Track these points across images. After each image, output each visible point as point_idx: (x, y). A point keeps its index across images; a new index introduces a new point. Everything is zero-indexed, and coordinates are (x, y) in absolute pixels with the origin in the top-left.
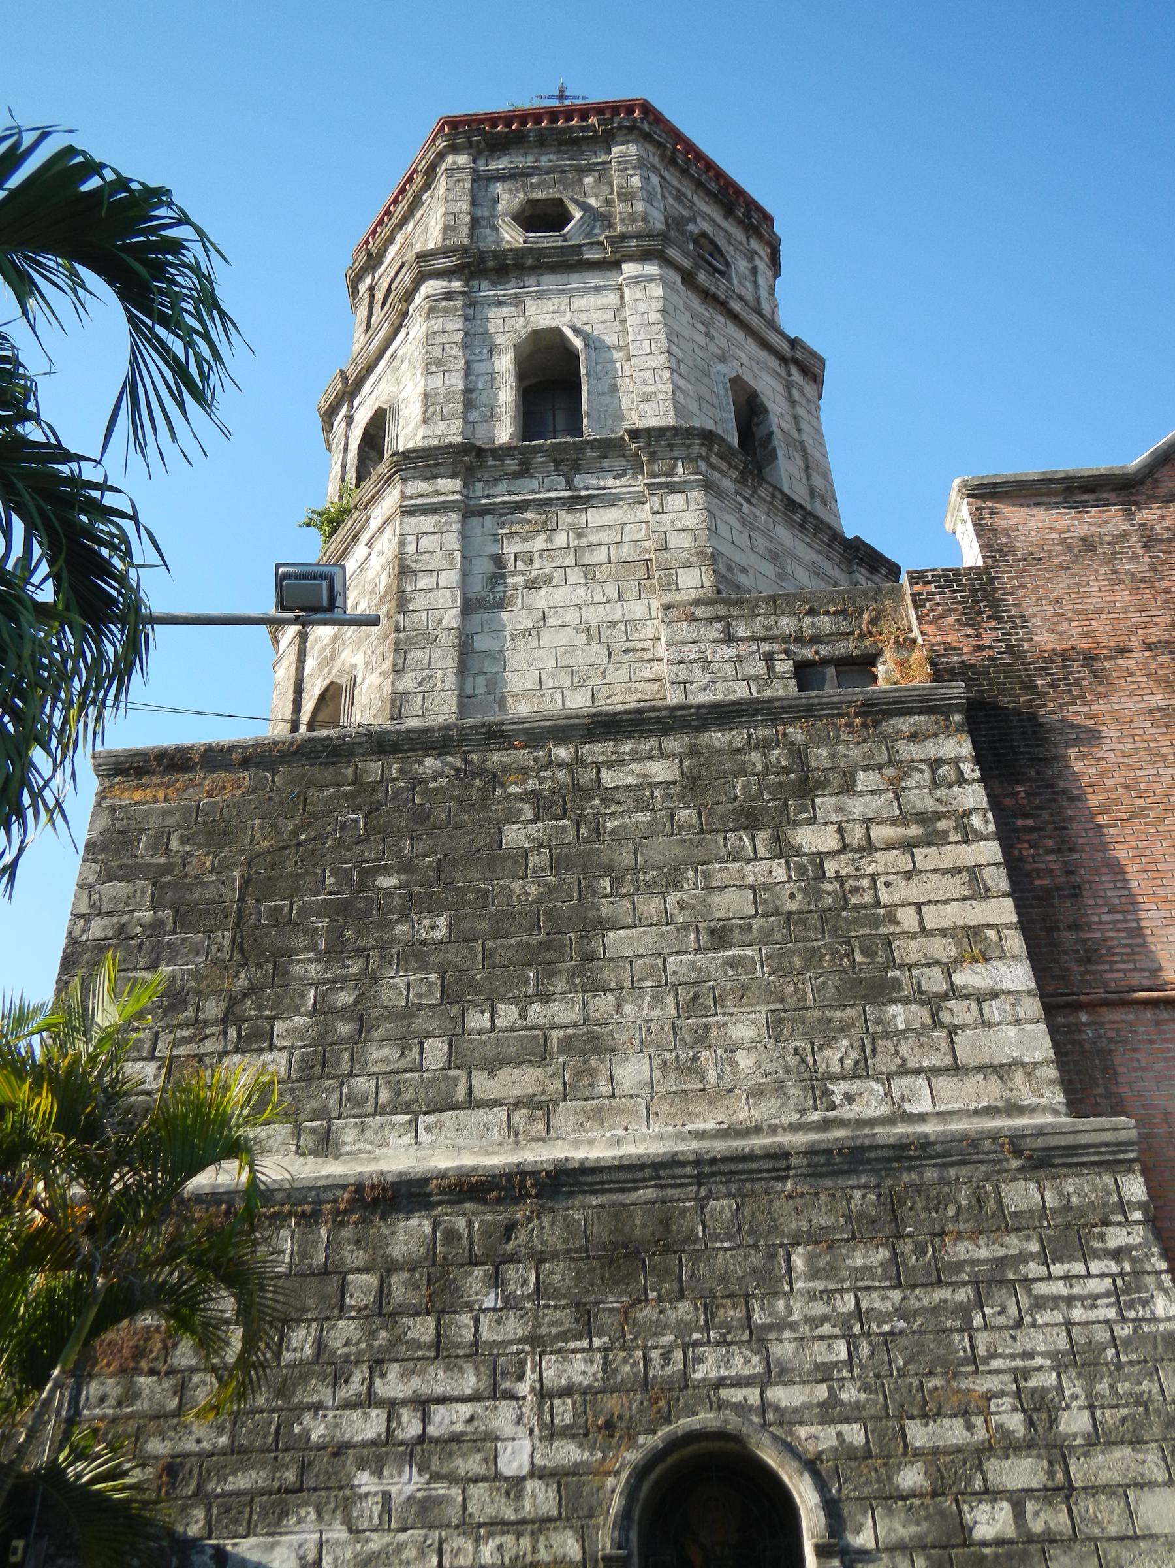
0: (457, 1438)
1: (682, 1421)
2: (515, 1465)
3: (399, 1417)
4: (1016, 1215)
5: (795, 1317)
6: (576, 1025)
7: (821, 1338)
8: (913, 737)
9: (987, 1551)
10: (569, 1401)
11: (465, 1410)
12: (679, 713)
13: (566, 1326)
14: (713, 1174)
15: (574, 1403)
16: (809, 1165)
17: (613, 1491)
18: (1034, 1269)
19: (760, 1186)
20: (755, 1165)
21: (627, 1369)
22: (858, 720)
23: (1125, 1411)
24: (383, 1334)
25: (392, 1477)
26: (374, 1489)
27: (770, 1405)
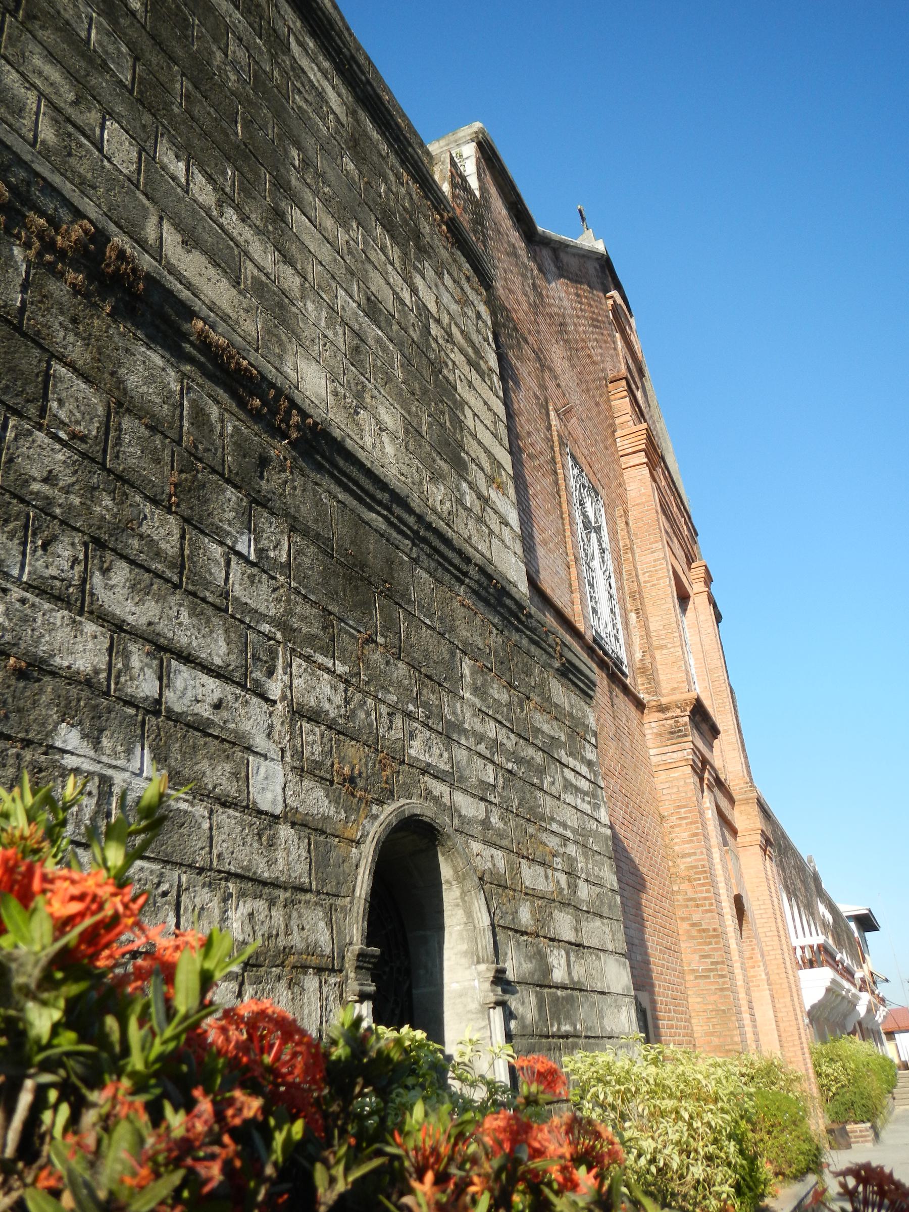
0: (200, 727)
1: (402, 801)
2: (269, 796)
3: (127, 656)
4: (557, 706)
5: (466, 726)
6: (267, 275)
7: (480, 755)
8: (468, 279)
9: (559, 993)
10: (317, 730)
11: (213, 688)
12: (354, 66)
13: (314, 631)
14: (425, 540)
15: (322, 736)
16: (478, 582)
17: (357, 866)
18: (562, 755)
19: (447, 577)
20: (450, 554)
21: (363, 716)
22: (444, 227)
23: (598, 890)
24: (107, 501)
25: (115, 754)
26: (87, 766)
27: (456, 810)
